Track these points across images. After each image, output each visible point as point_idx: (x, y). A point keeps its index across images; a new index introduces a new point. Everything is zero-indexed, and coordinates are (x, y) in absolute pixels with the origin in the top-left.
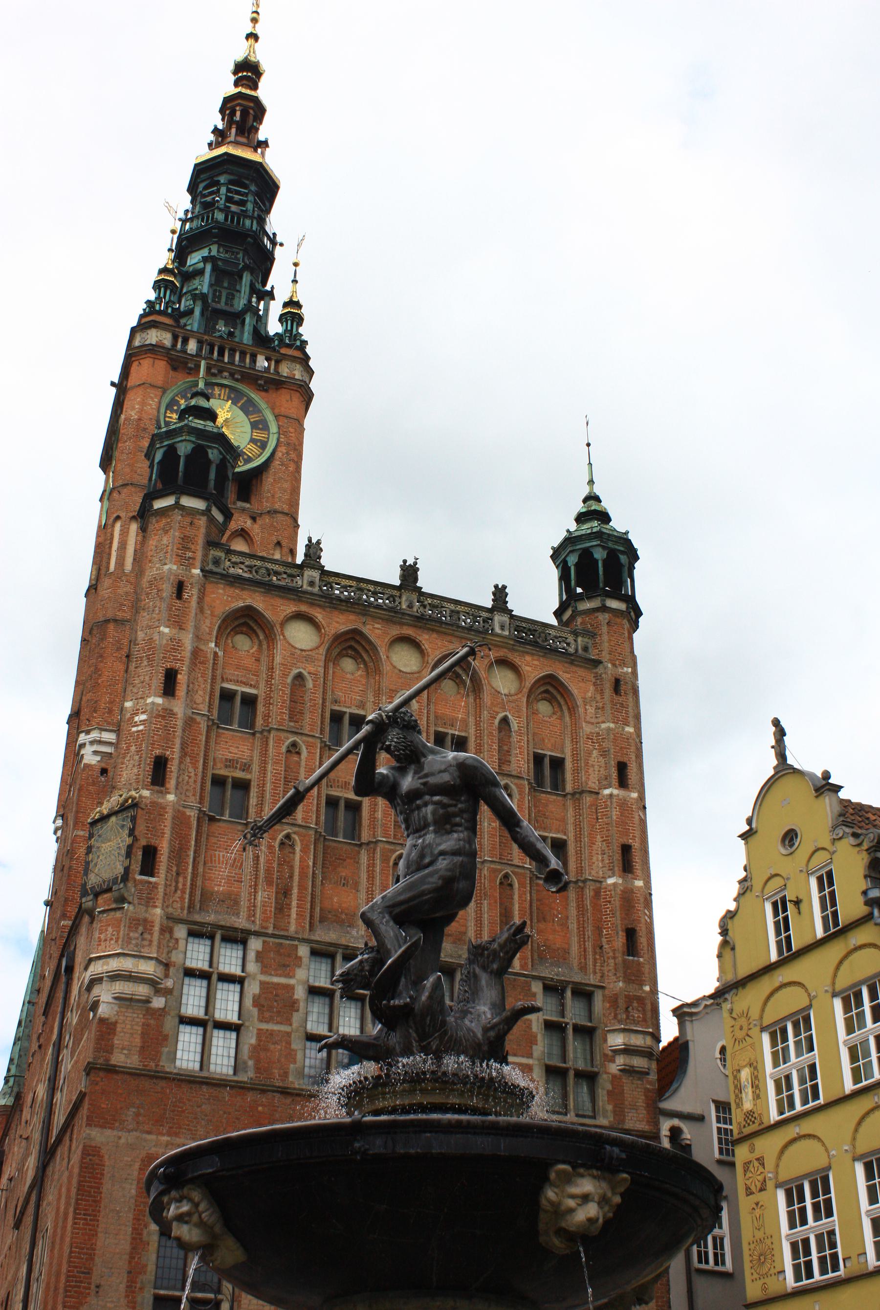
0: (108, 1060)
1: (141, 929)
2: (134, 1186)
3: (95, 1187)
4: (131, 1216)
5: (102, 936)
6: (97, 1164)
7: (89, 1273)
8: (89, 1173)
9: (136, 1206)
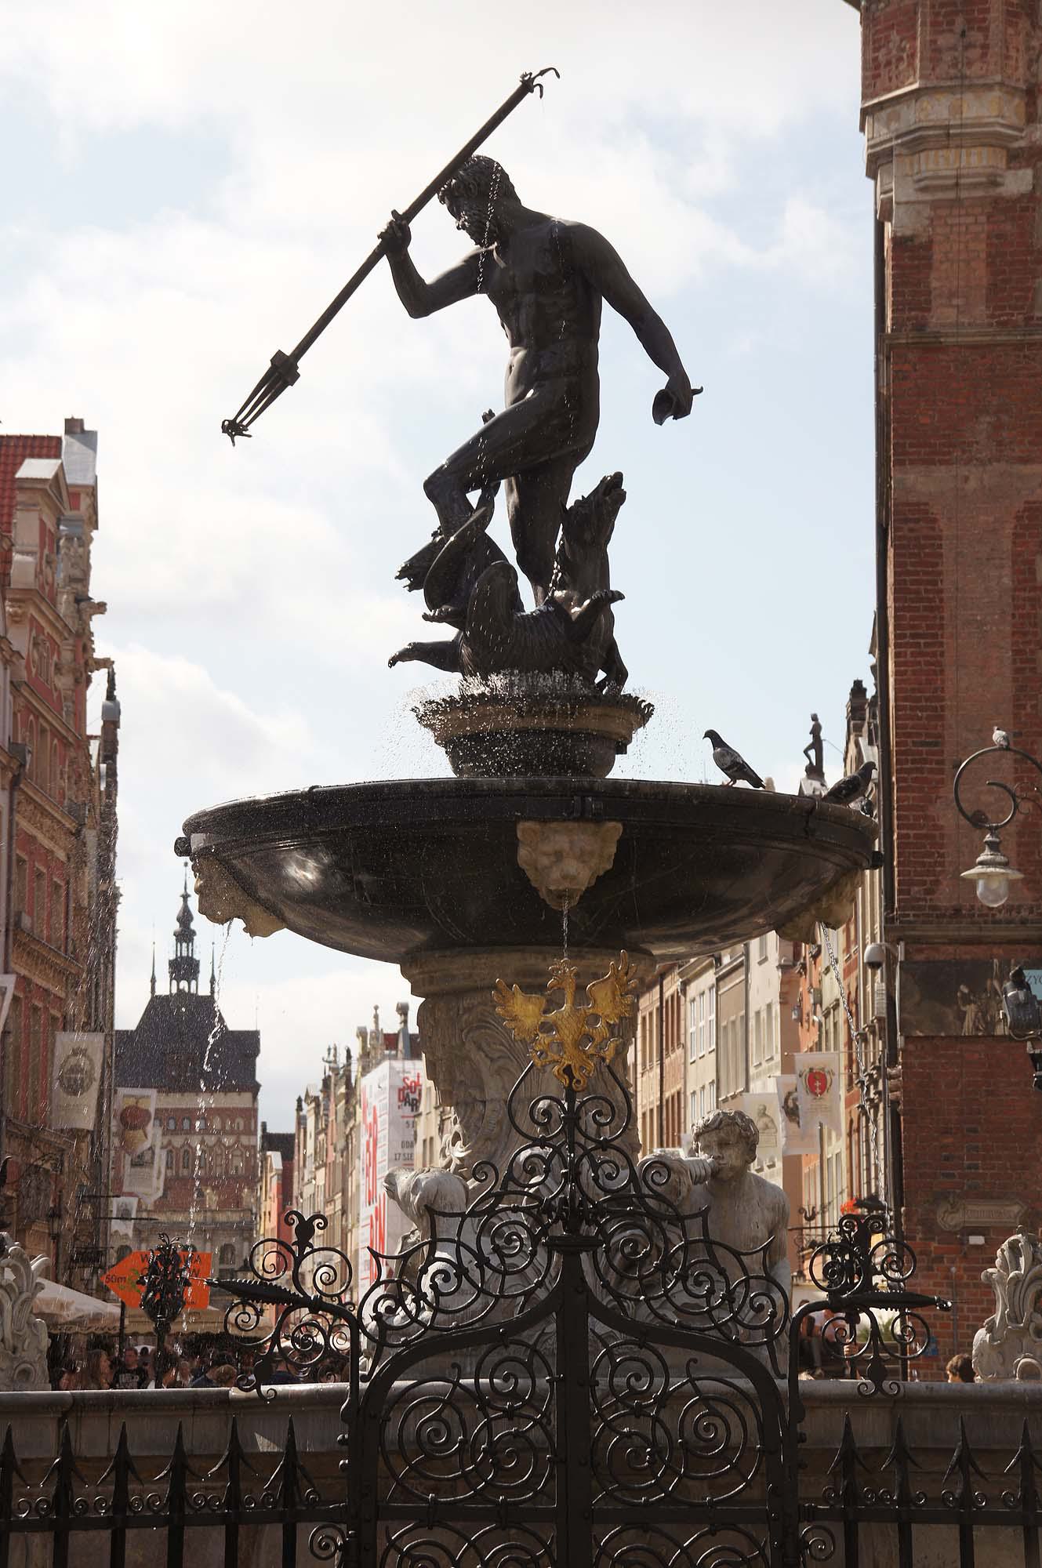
0: (920, 327)
1: (960, 22)
2: (1007, 571)
3: (929, 582)
4: (1008, 629)
5: (881, 55)
6: (926, 537)
7: (937, 741)
8: (912, 555)
9: (1016, 607)
